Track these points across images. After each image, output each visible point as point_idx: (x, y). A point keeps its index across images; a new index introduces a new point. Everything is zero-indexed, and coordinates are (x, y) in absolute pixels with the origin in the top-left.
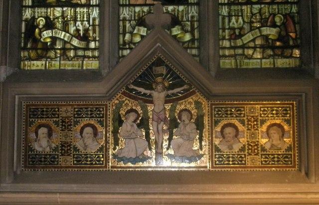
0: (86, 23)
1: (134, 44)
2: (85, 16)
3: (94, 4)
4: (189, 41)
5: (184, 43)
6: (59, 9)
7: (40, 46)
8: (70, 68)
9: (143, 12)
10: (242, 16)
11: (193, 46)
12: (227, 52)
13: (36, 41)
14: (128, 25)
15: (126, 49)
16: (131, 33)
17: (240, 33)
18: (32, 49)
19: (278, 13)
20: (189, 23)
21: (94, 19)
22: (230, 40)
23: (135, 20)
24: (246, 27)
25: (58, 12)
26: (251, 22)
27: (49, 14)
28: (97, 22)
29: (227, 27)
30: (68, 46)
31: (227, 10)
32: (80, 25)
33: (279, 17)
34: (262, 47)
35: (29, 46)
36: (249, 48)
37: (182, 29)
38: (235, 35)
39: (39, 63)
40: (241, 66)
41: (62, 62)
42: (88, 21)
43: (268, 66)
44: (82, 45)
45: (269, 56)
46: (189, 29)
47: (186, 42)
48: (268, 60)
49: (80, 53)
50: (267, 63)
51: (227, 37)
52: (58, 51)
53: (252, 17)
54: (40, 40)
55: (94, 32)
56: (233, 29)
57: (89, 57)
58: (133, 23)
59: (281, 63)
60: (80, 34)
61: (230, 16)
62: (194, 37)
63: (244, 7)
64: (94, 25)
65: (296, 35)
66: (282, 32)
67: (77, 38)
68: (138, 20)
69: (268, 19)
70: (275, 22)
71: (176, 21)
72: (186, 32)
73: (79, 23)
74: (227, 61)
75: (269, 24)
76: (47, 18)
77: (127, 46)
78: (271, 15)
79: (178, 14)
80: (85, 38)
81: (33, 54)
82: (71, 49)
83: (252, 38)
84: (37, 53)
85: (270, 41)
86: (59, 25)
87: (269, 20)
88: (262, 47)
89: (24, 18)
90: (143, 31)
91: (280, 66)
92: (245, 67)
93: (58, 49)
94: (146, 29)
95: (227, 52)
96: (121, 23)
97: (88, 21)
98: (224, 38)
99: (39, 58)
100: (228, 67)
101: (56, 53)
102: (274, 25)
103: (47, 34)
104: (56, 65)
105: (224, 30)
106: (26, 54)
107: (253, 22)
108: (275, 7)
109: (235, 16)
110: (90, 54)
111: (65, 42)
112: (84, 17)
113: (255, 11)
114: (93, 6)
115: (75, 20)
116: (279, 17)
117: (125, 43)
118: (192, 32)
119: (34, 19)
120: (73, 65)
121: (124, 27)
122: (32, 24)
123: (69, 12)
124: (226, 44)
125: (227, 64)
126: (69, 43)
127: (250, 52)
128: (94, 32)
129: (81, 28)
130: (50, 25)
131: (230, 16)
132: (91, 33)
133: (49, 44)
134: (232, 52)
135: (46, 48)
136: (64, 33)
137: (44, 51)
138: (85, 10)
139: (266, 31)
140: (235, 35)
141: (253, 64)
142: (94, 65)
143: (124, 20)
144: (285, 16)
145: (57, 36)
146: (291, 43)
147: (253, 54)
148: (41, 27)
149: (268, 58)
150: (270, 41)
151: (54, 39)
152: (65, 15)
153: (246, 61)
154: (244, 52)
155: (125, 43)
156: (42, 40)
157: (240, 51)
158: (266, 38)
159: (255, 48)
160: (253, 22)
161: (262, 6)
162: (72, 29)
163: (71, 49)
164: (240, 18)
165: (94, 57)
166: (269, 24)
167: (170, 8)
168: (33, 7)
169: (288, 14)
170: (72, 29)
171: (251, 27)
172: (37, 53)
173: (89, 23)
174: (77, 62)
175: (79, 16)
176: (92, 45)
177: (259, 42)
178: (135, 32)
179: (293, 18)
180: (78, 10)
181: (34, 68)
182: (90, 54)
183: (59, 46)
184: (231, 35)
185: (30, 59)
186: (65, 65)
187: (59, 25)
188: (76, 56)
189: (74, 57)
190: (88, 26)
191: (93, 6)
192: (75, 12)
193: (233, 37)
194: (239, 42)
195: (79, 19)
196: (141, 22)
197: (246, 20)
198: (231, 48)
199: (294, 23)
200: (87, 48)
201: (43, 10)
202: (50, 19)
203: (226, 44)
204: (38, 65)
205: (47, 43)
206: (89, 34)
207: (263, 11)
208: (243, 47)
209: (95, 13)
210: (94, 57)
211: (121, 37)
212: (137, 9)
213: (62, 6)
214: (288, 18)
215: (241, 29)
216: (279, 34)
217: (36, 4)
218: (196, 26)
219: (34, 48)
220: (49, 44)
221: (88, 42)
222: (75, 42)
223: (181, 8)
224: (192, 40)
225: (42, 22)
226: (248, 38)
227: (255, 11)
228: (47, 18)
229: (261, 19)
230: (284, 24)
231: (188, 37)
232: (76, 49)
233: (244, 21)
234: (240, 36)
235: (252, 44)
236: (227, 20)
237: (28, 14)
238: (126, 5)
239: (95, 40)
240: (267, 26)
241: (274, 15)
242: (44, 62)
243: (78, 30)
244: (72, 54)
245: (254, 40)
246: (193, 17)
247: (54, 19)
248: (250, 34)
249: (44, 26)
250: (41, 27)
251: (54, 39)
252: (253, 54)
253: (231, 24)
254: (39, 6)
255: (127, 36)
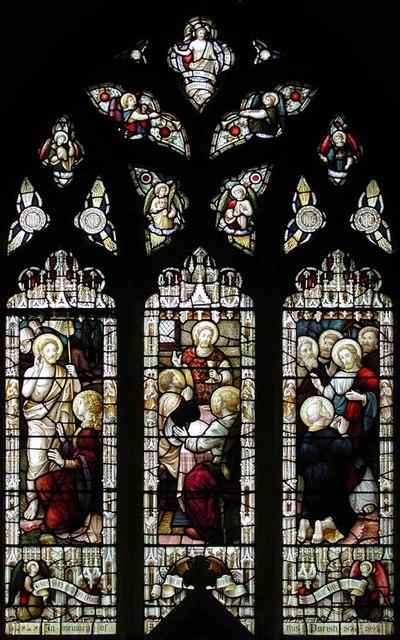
0: (98, 569)
1: (165, 600)
2: (96, 560)
3: (108, 543)
4: (240, 597)
5: (234, 599)
6: (58, 549)
7: (32, 601)
8: (76, 633)
9: (177, 554)
10: (315, 563)
11: (247, 604)
12: (293, 613)
13: (27, 595)
14: (156, 573)
15: (154, 606)
16: (161, 584)
17: (311, 586)
18: (21, 605)
19: (366, 560)
20: (241, 572)
21: (108, 565)
22: (297, 595)
23: (166, 566)
24: (321, 578)
25: (56, 553)
26: (328, 572)
27: (44, 556)
28: (113, 569)
29: (294, 578)
30: (72, 602)
31: (294, 553)
32: (89, 572)
33: (366, 565)
34: (342, 606)
35: (17, 601)
36: (324, 607)
37: (232, 579)
38: (305, 590)
39: (30, 625)
40: (312, 631)
41: (64, 624)
42: (101, 567)
43: (349, 633)
44: (92, 600)
45: (352, 619)
46: (242, 580)
47: (237, 598)
48: (349, 624)
49: (89, 611)
50: (347, 630)
51: (293, 592)
52: (59, 609)
53: (328, 564)
54: (31, 594)
55: (109, 582)
56: (303, 581)
57: (102, 618)
58: (164, 570)
59: (368, 628)
60: (88, 585)
61: (298, 562)
62: (248, 591)
63: (318, 550)
64: (108, 573)
65: (389, 590)
66: (370, 586)
67: (84, 590)
68: (170, 567)
69: (351, 567)
70: (360, 572)
71: (224, 569)
72: (237, 583)
73: (86, 570)
74: (292, 625)
75: (352, 574)
76: (41, 562)
77: (155, 603)
78: (355, 561)
79: (226, 558)
80: (96, 590)
81: (22, 612)
82: (76, 606)
83: (328, 593)
84: (29, 611)
85: (353, 598)
86: (59, 572)
87: (353, 568)
88: (342, 606)
89: (8, 562)
90: (177, 581)
91: (366, 633)
92: (317, 633)
93: (57, 606)
94: (181, 579)
95: (293, 613)
96: (146, 570)
97: (101, 567)
98: (289, 593)
99: (31, 618)
100: (295, 633)
101: (55, 611)
102: (358, 576)
103: (41, 587)
104: (54, 628)
105: (289, 581)
106: (13, 612)
107: (330, 572)
108: (361, 550)
109: (305, 562)
110: (102, 612)
111: (68, 597)
112: (93, 561)
113: (333, 556)
114: (106, 546)
115: (82, 566)
116: (366, 565)
117: (152, 599)
118: (245, 584)
119: (22, 562)
120: (79, 629)
121: (151, 576)
122: (20, 572)
123: (72, 553)
124: (293, 601)
125: (291, 628)
126: (74, 597)
127: (326, 612)
128: (109, 582)
129: (89, 576)
130: (45, 572)
131: (298, 562)
132: (104, 583)
133: (45, 598)
134: (300, 612)
135: (41, 605)
136: (65, 583)
137: (38, 608)
138: (95, 550)
139: (347, 584)
140: (305, 590)
141: (330, 629)
142: (110, 628)
143: (151, 566)
144: (375, 563)
145: (56, 588)
146: (382, 601)
147: (329, 615)
148: (32, 575)
149: (350, 622)
150: (353, 598)
151: (52, 592)
152: (67, 558)
153: (319, 625)
154: (316, 612)
155: (152, 599)
156: (35, 593)
157: (311, 611)
158: (347, 594)
159: (331, 608)
160: (330, 572)
161: (344, 549)
162: (77, 578)
163: (76, 606)
164: (313, 565)
165: (110, 618)
166: (352, 574)
167: (216, 550)
168: (20, 546)
169: (379, 562)
170: (77, 578)
171: (327, 578)
172: (29, 611)
173: (101, 570)
174: (85, 625)
175: (87, 561)
176: (106, 601)
177: (337, 599)
178: (166, 583)
179: (385, 567)
180: (85, 550)
181: (24, 633)
182: (102, 612)
183: (59, 600)
184: (299, 589)
185: (18, 620)
186: (68, 629)
187: (59, 572)
188: (83, 616)
189: (81, 617)
190: (100, 574)
191: (106, 546)
192: (82, 555)
193: (302, 591)
194: (310, 599)
195: (86, 564)
196: (174, 570)
197: (320, 568)
198: (300, 606)
199: (387, 575)
200: (99, 606)
201: (36, 550)
202: (45, 563)
203: (293, 601)
204: (31, 628)
205: (42, 597)
206: (102, 585)
207: (344, 556)
208: (315, 605)
209: (110, 555)
210: (110, 618)
211: (147, 589)
212: (169, 551)
213: (63, 546)
214: (380, 567)
215: (314, 580)
216: (366, 589)
217: (24, 542)
218: (251, 577)
219: (24, 605)
220: (45, 598)
221: (101, 595)
222: (83, 596)
223: (231, 550)
224: (246, 596)
225: (33, 568)
226: (322, 593)
227: (333, 556)
228: (41, 562)
229: (342, 567)
230: (372, 576)
231: (239, 591)
232: (83, 605)
233: (317, 570)
234: (312, 590)
235: (328, 603)
236: (294, 567)
237: (12, 556)
238: (153, 546)
239: (109, 593)
240: (349, 577)
241: (360, 562)
242: (38, 625)
243: (85, 580)
244: (77, 612)
245: (330, 597)
246: (246, 563)
247: (51, 564)
248: (325, 588)
249: (37, 574)
250: (32, 575)
251: (52, 592)
252: (329, 615)
253: (299, 574)
254: (27, 546)
255: (156, 589)
